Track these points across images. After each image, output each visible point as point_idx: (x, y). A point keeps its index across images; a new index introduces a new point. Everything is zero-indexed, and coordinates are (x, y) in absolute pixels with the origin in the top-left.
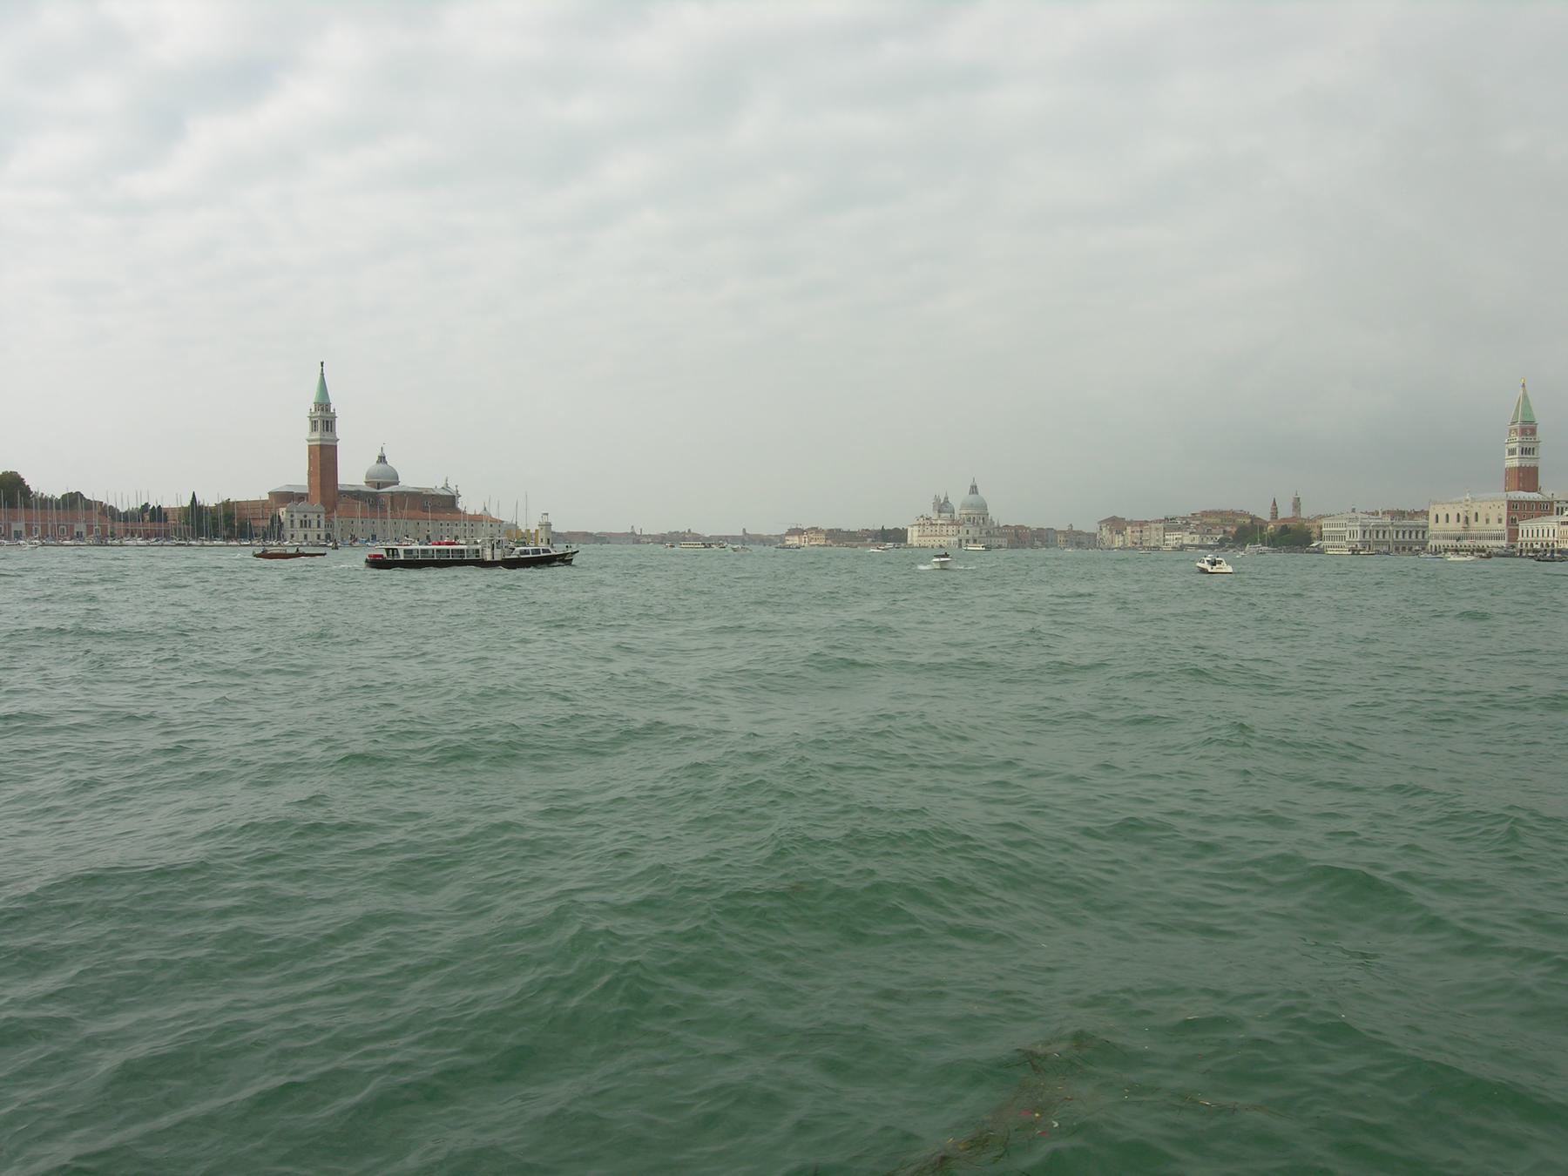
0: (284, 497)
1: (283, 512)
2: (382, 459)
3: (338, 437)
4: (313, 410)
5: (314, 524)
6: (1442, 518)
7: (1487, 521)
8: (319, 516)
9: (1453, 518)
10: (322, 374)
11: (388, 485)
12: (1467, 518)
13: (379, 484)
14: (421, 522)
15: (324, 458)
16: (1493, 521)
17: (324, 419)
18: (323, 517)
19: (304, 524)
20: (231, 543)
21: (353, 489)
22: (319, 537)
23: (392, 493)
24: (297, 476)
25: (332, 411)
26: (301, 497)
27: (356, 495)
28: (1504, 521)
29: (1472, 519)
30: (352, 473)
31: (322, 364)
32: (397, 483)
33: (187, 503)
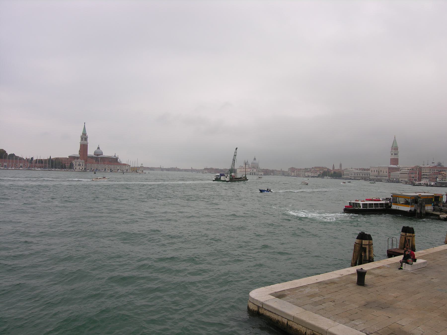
0: (73, 158)
1: (74, 162)
2: (99, 148)
3: (88, 142)
4: (82, 135)
5: (82, 165)
6: (373, 171)
7: (384, 172)
8: (83, 163)
9: (375, 171)
10: (85, 126)
11: (100, 155)
12: (379, 171)
13: (97, 155)
14: (109, 165)
15: (84, 148)
16: (385, 173)
17: (84, 137)
18: (84, 163)
19: (79, 165)
20: (56, 170)
21: (91, 156)
22: (83, 168)
23: (101, 157)
24: (76, 152)
25: (87, 135)
26: (78, 158)
27: (92, 157)
28: (387, 172)
29: (380, 171)
30: (91, 152)
31: (85, 123)
32: (102, 155)
33: (49, 158)
